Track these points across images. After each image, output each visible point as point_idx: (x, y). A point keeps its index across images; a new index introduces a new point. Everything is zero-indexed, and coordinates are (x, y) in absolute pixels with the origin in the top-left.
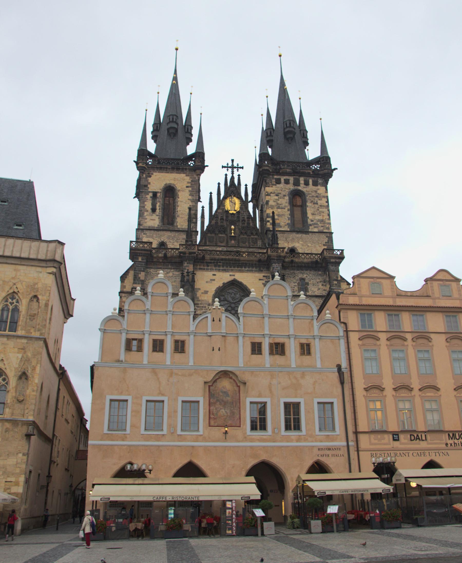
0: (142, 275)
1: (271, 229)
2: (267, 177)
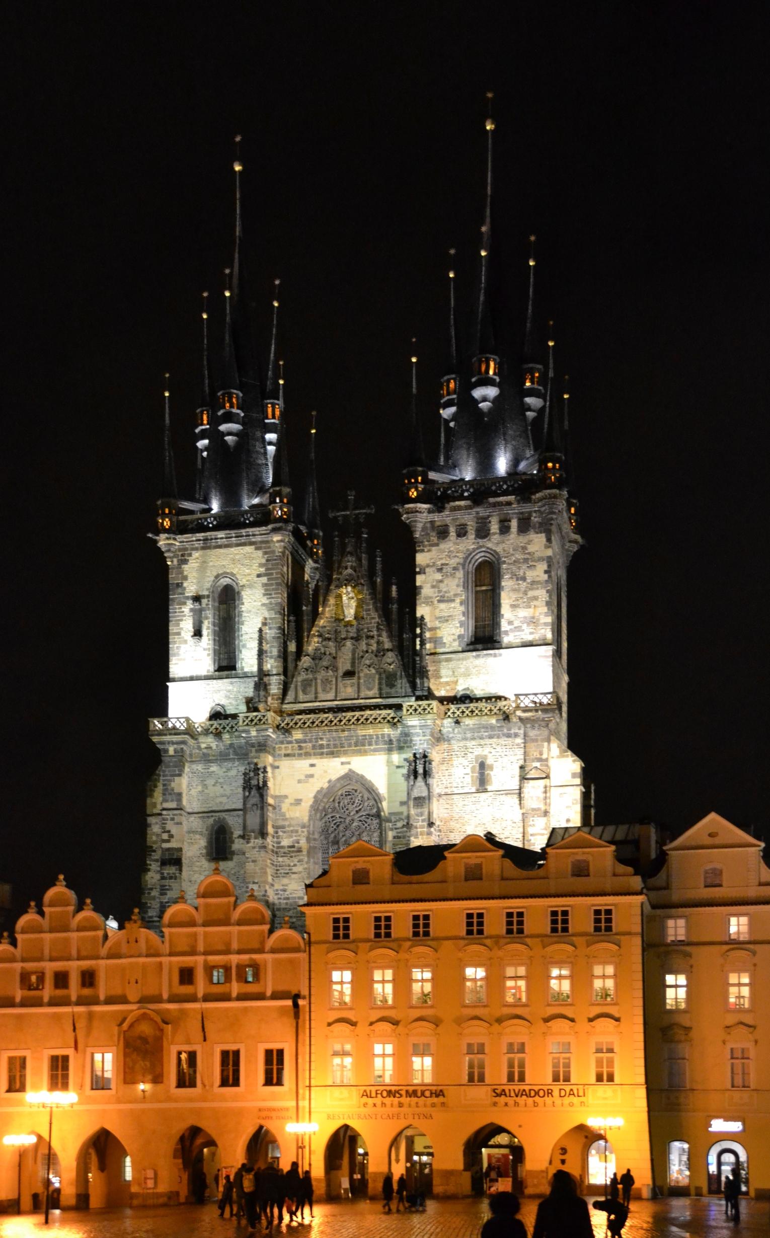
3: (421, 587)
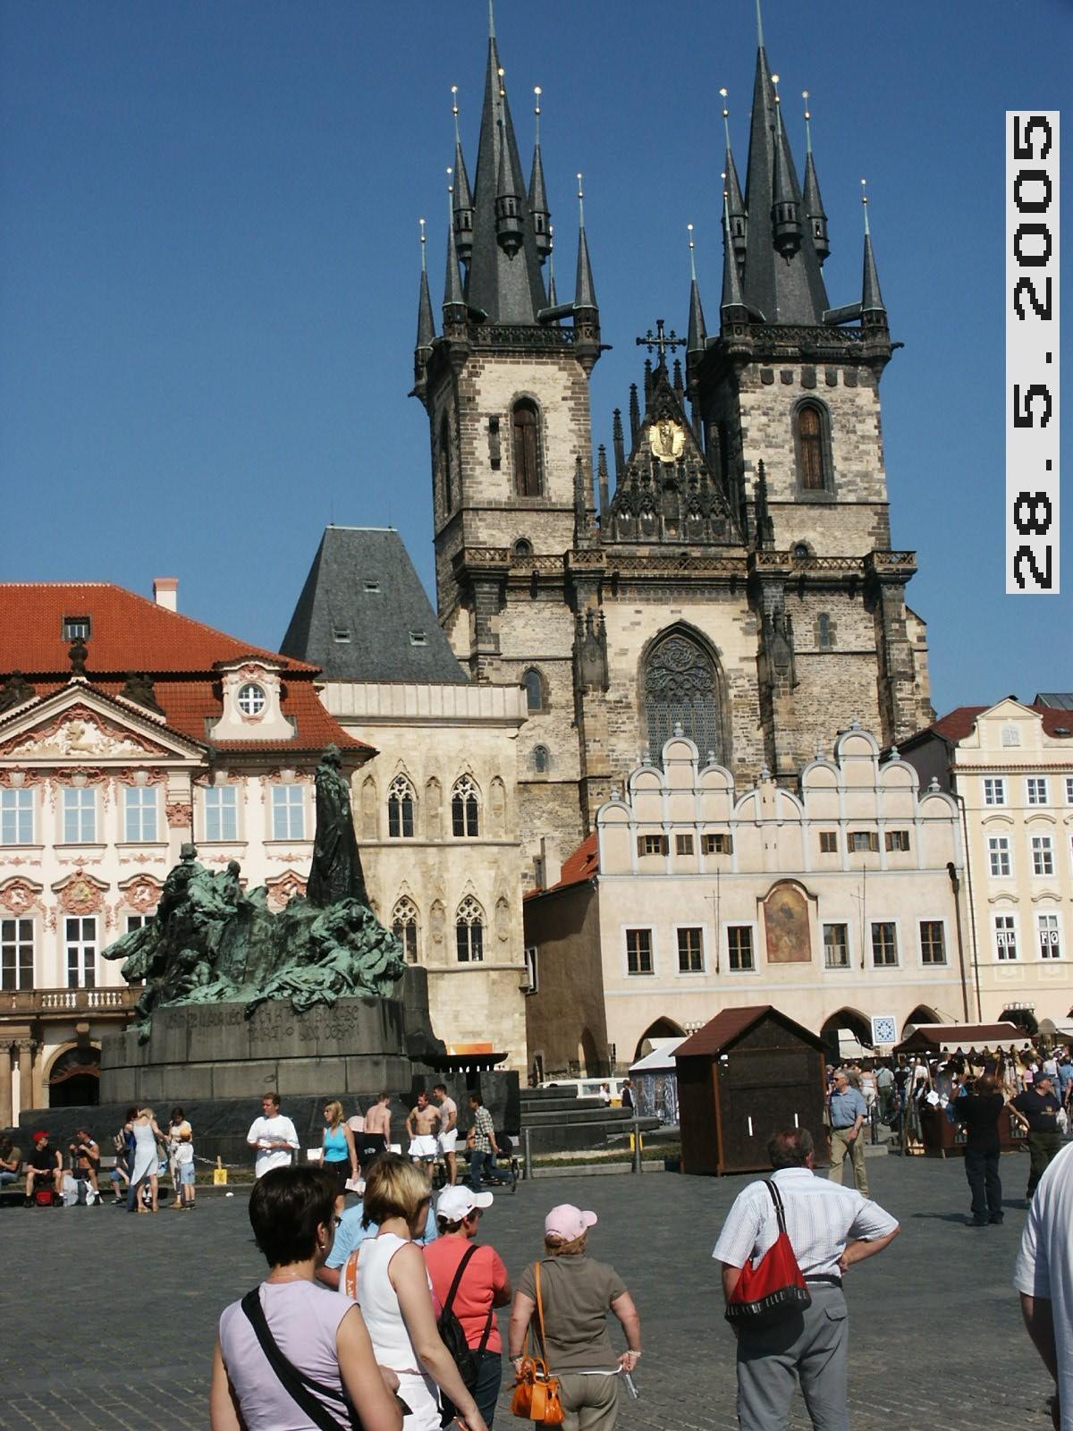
0: (495, 623)
1: (754, 500)
2: (741, 369)
3: (747, 429)
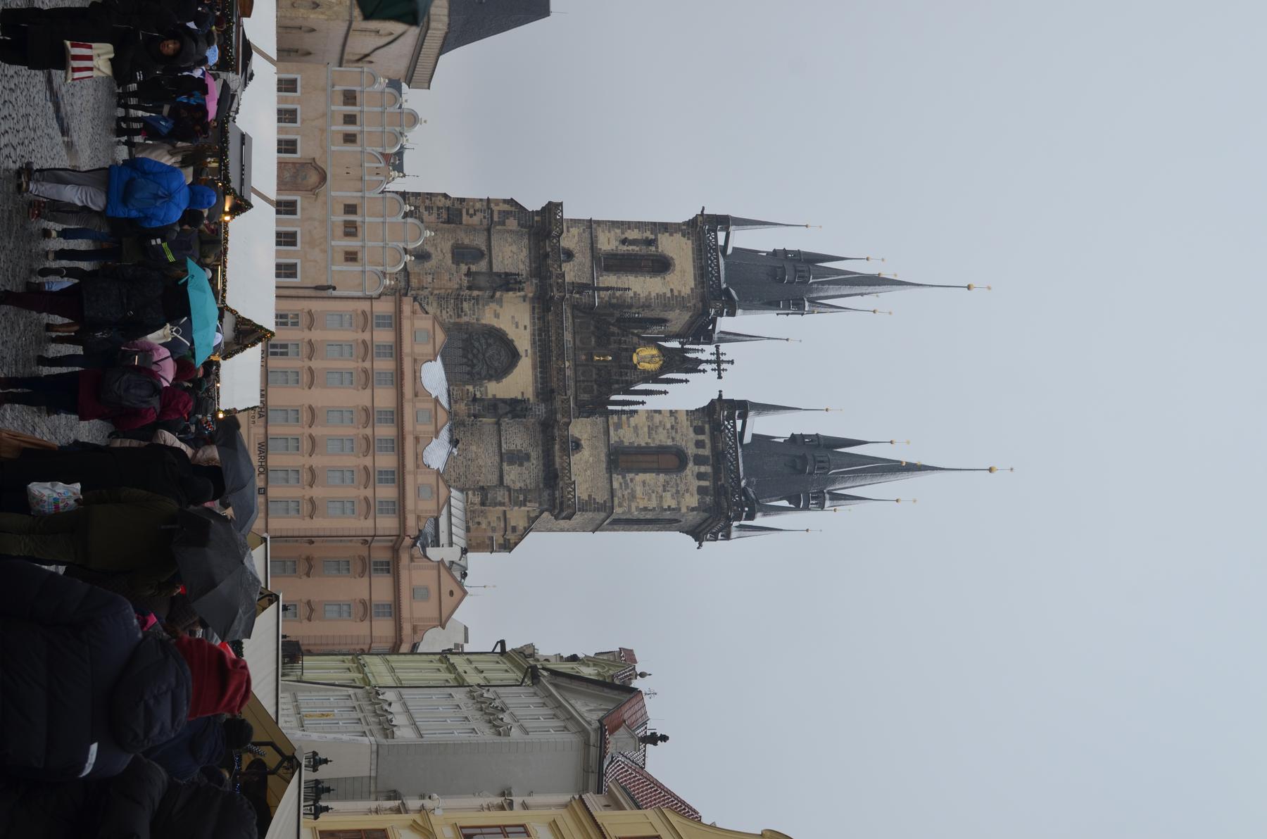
0: (512, 223)
